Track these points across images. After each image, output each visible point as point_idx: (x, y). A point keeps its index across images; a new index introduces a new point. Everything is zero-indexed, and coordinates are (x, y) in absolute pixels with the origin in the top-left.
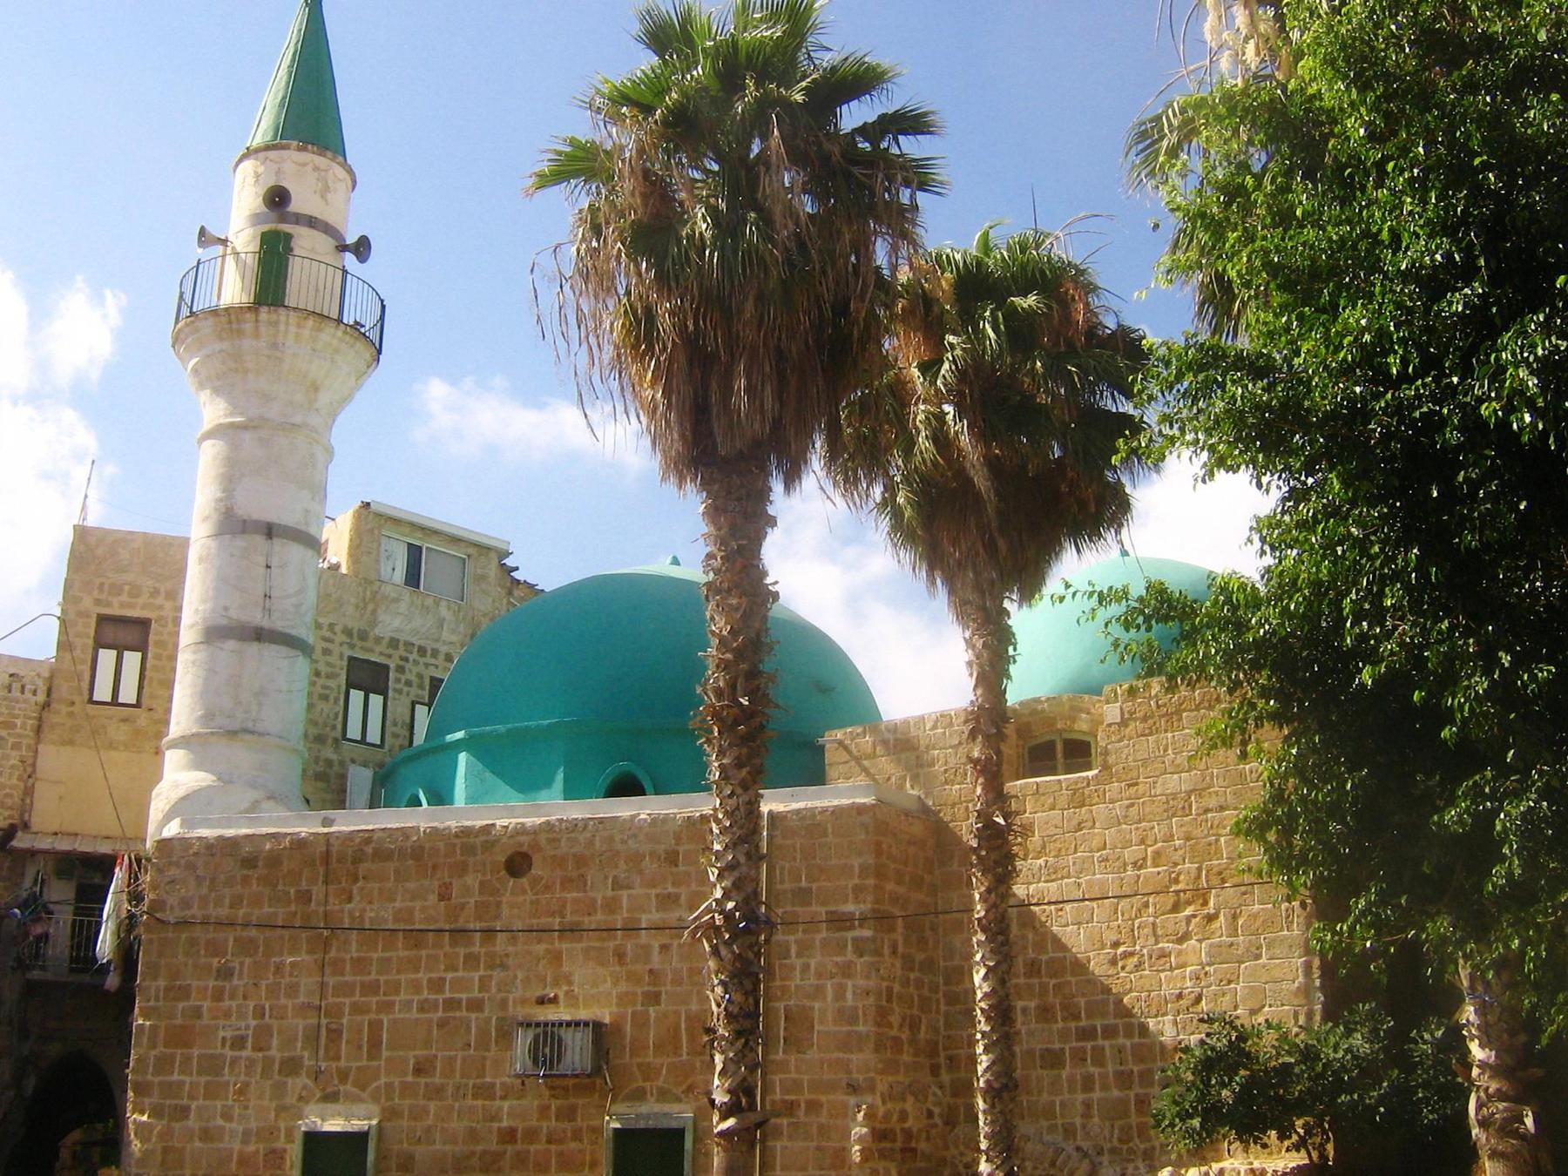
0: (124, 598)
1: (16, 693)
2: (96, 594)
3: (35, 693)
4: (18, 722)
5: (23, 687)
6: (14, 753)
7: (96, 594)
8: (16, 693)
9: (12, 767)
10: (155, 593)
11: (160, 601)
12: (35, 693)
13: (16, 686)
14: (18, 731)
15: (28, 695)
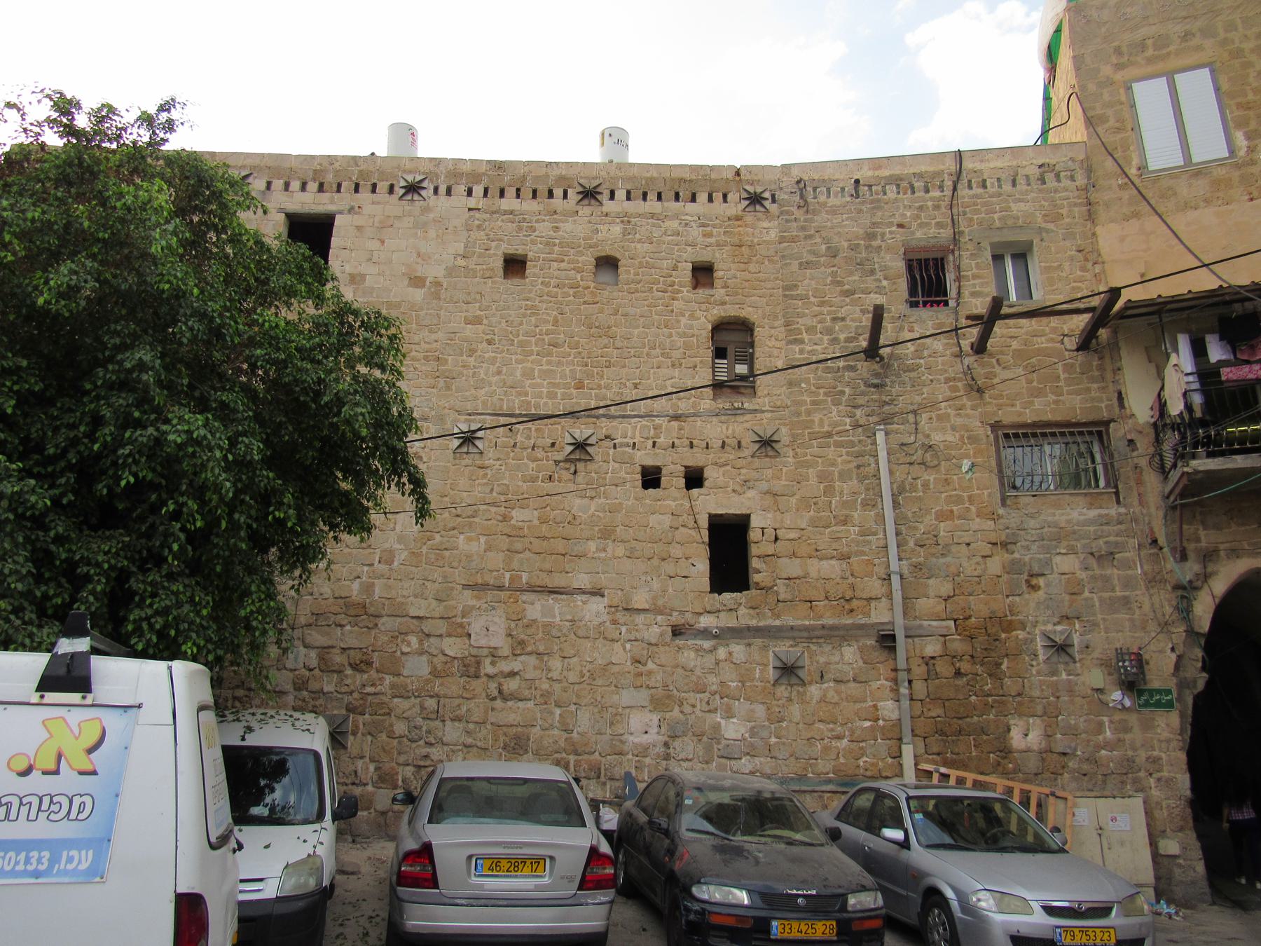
0: (1150, 52)
1: (1051, 183)
2: (1114, 60)
3: (1072, 178)
4: (1064, 212)
5: (1057, 176)
6: (1068, 243)
7: (1114, 60)
8: (1051, 183)
9: (1072, 259)
10: (1187, 36)
11: (1196, 41)
12: (1072, 178)
13: (1049, 177)
14: (1068, 220)
15: (1066, 183)
